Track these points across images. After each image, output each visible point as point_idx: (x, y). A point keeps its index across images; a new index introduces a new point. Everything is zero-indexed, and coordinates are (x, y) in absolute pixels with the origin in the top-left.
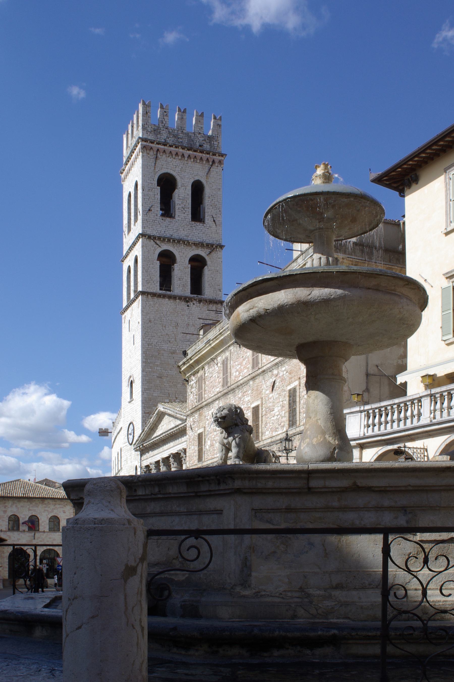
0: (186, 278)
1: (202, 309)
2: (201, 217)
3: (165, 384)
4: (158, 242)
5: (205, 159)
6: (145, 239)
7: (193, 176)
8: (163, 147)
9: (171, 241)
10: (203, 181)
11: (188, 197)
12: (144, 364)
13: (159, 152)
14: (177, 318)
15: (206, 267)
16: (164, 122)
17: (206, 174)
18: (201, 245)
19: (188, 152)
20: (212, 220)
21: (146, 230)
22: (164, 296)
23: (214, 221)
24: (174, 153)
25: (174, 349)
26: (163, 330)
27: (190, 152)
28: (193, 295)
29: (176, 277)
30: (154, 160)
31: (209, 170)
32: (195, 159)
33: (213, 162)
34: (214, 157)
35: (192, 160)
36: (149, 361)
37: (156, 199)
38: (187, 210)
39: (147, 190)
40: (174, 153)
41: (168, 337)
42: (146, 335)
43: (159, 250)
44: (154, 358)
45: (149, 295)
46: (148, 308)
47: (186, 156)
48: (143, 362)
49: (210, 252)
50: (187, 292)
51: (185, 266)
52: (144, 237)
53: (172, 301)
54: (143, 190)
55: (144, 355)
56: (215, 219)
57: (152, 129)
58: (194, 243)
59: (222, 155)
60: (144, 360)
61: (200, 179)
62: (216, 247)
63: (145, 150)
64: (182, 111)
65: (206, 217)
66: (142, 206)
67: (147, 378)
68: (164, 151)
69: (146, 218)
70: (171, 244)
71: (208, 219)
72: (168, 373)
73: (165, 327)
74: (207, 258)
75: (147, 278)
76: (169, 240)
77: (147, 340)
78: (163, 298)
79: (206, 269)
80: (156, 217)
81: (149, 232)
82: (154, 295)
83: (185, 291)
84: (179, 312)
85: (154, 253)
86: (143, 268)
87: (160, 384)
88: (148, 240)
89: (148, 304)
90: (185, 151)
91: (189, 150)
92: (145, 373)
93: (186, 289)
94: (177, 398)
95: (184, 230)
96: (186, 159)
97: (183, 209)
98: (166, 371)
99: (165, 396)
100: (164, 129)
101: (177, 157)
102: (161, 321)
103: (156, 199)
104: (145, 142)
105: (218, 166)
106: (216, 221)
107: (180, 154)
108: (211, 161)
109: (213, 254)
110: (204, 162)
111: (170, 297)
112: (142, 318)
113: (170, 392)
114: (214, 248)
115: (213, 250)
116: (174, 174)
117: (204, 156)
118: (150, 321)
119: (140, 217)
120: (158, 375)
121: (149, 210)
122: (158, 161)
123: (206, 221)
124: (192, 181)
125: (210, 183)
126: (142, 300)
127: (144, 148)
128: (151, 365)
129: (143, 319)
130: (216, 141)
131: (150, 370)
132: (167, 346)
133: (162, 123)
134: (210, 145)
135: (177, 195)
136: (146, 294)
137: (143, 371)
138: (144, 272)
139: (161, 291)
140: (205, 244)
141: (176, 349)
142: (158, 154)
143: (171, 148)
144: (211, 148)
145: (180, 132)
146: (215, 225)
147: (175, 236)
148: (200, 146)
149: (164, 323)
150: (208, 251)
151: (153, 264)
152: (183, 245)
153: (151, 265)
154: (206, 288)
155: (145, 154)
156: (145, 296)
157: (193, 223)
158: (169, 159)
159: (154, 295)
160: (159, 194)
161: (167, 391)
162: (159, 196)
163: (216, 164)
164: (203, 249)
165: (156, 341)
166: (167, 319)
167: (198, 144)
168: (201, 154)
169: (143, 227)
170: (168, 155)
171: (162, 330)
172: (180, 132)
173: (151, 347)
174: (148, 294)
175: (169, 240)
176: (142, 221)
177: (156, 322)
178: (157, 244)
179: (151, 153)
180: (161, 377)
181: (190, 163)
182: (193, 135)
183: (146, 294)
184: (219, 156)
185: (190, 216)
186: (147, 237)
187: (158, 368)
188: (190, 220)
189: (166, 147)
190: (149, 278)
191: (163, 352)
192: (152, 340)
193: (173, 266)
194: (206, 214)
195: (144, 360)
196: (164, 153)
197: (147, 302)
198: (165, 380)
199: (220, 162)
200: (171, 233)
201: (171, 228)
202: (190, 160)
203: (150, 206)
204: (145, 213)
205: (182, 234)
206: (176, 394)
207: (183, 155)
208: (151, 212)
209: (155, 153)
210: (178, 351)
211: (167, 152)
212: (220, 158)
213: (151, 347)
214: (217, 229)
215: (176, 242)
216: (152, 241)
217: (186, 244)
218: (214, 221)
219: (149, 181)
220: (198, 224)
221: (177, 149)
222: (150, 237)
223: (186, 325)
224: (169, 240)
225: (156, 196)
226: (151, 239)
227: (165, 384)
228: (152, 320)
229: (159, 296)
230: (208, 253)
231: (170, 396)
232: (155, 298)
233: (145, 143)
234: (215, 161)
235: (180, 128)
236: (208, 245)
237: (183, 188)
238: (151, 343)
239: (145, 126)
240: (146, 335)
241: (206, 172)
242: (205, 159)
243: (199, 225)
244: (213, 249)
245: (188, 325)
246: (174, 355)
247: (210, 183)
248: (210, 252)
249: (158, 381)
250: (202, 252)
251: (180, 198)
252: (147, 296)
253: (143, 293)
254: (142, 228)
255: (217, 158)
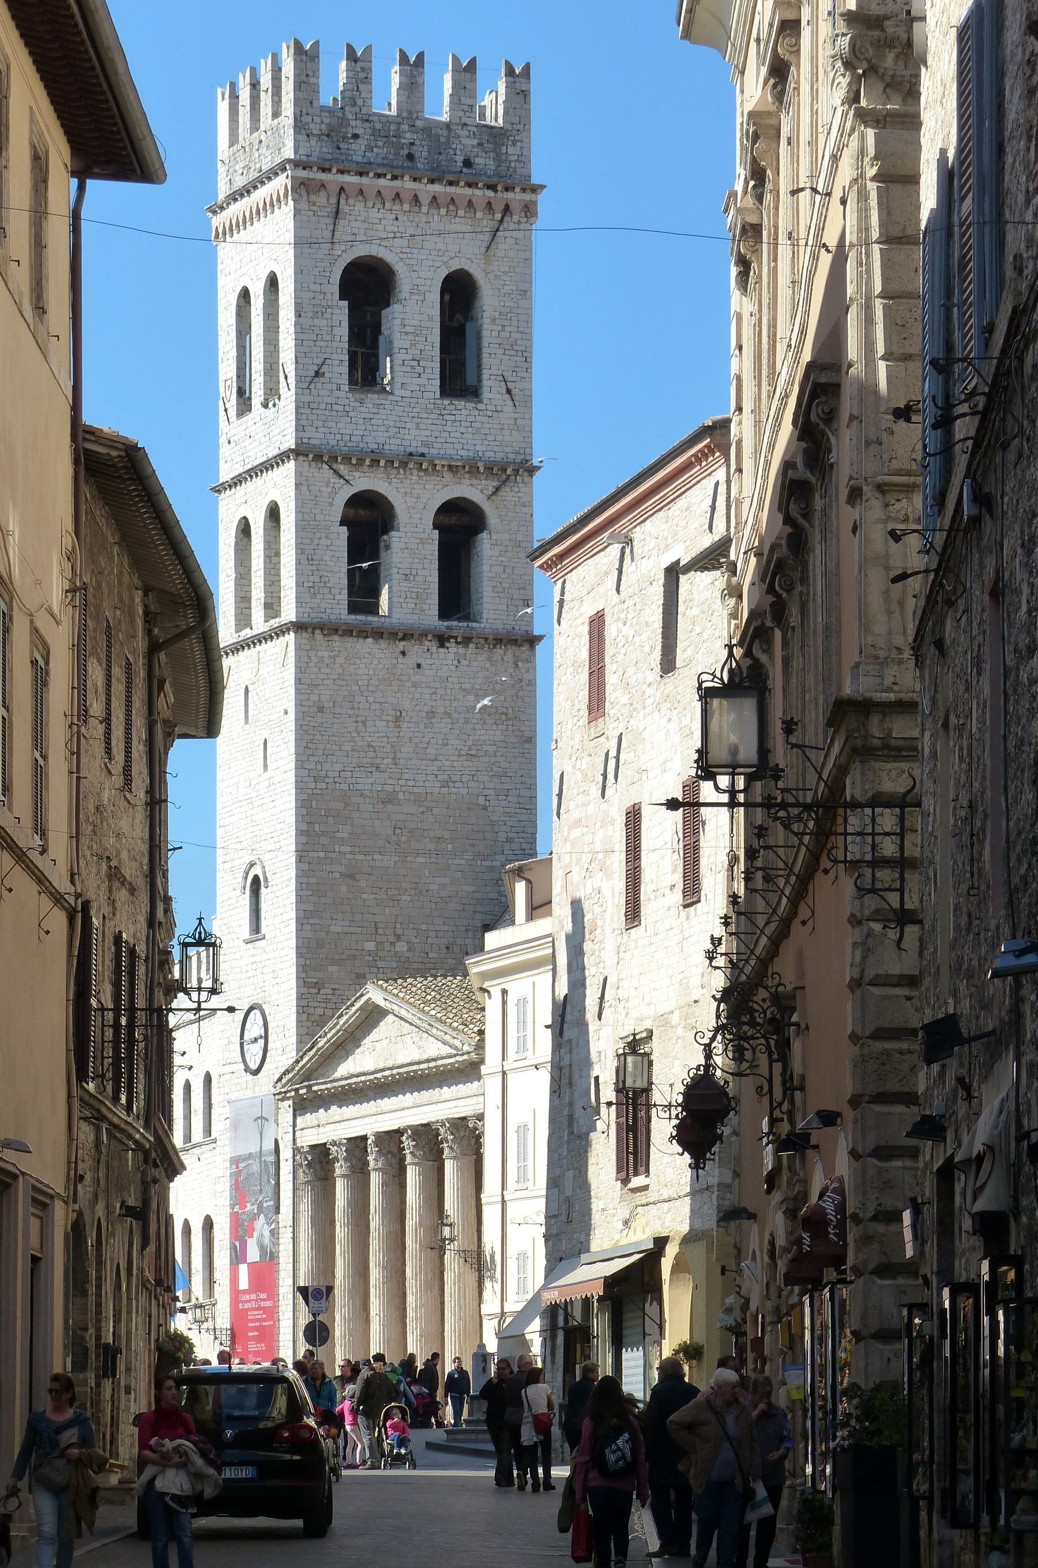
0: (426, 573)
1: (475, 664)
2: (471, 380)
3: (364, 896)
4: (343, 469)
5: (480, 204)
6: (306, 464)
7: (445, 259)
8: (355, 179)
9: (382, 463)
10: (476, 271)
11: (429, 324)
12: (304, 839)
13: (343, 195)
14: (399, 695)
15: (484, 535)
16: (360, 102)
17: (483, 250)
18: (470, 468)
19: (431, 187)
20: (504, 391)
21: (305, 435)
22: (363, 633)
23: (509, 391)
24: (388, 195)
25: (390, 788)
26: (358, 733)
27: (437, 188)
28: (446, 624)
29: (395, 570)
30: (330, 221)
31: (495, 236)
32: (451, 207)
33: (507, 210)
34: (510, 195)
35: (443, 211)
36: (317, 829)
37: (337, 339)
38: (430, 364)
39: (310, 315)
40: (388, 195)
41: (372, 754)
42: (310, 752)
43: (347, 493)
44: (331, 819)
45: (318, 632)
46: (316, 670)
47: (425, 200)
48: (300, 833)
49: (497, 489)
50: (429, 614)
51: (422, 536)
52: (301, 458)
53: (383, 644)
54: (298, 315)
55: (304, 811)
56: (510, 386)
57: (323, 127)
58: (450, 466)
59: (535, 189)
60: (305, 827)
61: (466, 268)
62: (516, 472)
63: (304, 193)
64: (412, 59)
65: (486, 383)
66: (297, 362)
67: (314, 880)
68: (361, 192)
69: (308, 399)
70: (380, 473)
71: (491, 389)
72: (372, 863)
73: (364, 723)
74: (487, 507)
75: (311, 578)
76: (374, 459)
77: (312, 766)
78: (358, 637)
79: (485, 541)
80: (336, 393)
81: (316, 438)
82: (331, 629)
83: (423, 610)
84: (404, 678)
85: (331, 504)
86: (300, 550)
87: (350, 896)
88: (313, 464)
89: (313, 658)
90: (422, 186)
91: (432, 181)
92: (306, 867)
93: (425, 607)
94: (398, 937)
95: (418, 428)
96: (424, 209)
97: (415, 363)
98: (369, 858)
99: (365, 931)
100: (359, 123)
101: (397, 207)
102: (353, 708)
103: (337, 339)
104: (304, 168)
105: (519, 223)
106: (514, 392)
107: (406, 196)
108: (499, 208)
109: (508, 494)
110: (479, 215)
111: (378, 634)
112: (296, 700)
113: (377, 918)
114: (509, 476)
115: (504, 482)
116: (389, 257)
117: (480, 194)
118: (321, 709)
119: (288, 397)
120: (342, 869)
121: (317, 374)
122: (342, 222)
123: (486, 394)
124: (443, 274)
125: (497, 277)
126: (298, 648)
127: (301, 189)
128: (324, 840)
129: (299, 704)
130: (514, 144)
131: (322, 854)
132: (371, 780)
133: (354, 104)
134: (498, 160)
135: (397, 322)
136: (310, 630)
137: (300, 858)
138: (304, 561)
139: (353, 617)
140: (481, 465)
141: (398, 788)
142: (342, 202)
143: (382, 182)
144: (499, 166)
145: (405, 127)
146: (510, 403)
147: (394, 446)
148: (468, 163)
149: (361, 712)
150: (491, 484)
151: (327, 538)
152: (415, 472)
153: (324, 542)
154: (485, 599)
155: (304, 205)
156: (305, 634)
157: (446, 402)
158: (375, 214)
159: (331, 629)
160: (345, 324)
161: (370, 917)
162: (344, 331)
163: (515, 218)
164: (476, 482)
165: (338, 767)
166: (371, 699)
167: (460, 159)
168: (468, 191)
169: (300, 428)
170: (370, 204)
171: (354, 734)
172: (405, 127)
173: (324, 786)
174: (314, 629)
175: (375, 462)
176: (297, 408)
177: (338, 710)
178: (341, 476)
179: (321, 199)
180: (352, 877)
181: (437, 220)
182: (445, 133)
183: (310, 630)
184: (524, 190)
185: (438, 382)
186: (311, 456)
187: (343, 849)
188: (438, 395)
189: (364, 180)
190: (317, 579)
191: (360, 800)
192: (327, 766)
193: (385, 537)
194: (486, 374)
195: (305, 827)
196: (360, 198)
197: (312, 653)
198: (363, 884)
199: (529, 210)
200: (381, 440)
201: (380, 422)
202: (435, 211)
203: (319, 361)
204: (305, 385)
205: (413, 439)
206: (398, 926)
207: (416, 200)
208: (322, 379)
209: (333, 200)
210: (401, 796)
211: (371, 193)
212: (527, 197)
213: (324, 786)
214: (516, 415)
215: (396, 465)
216: (325, 466)
217: (426, 470)
218: (509, 391)
219: (316, 287)
220: (460, 404)
221: (397, 183)
222: (318, 458)
223: (425, 714)
224: (374, 459)
225: (336, 331)
226: (323, 462)
227: (364, 896)
228: (326, 704)
229: (348, 632)
230: (491, 489)
231: (380, 931)
232: (336, 637)
233: (304, 174)
234: (511, 206)
235: (405, 114)
236: (489, 469)
237: (416, 297)
238: (323, 774)
239: (304, 119)
240: (310, 752)
241: (485, 244)
242: (480, 204)
243: (463, 407)
244: (504, 477)
245: (432, 714)
246: (390, 808)
247: (497, 277)
248: (497, 489)
249: (344, 889)
250: (473, 491)
251: (408, 329)
252: (313, 633)
253: (298, 627)
254: (297, 430)
255: (516, 197)
